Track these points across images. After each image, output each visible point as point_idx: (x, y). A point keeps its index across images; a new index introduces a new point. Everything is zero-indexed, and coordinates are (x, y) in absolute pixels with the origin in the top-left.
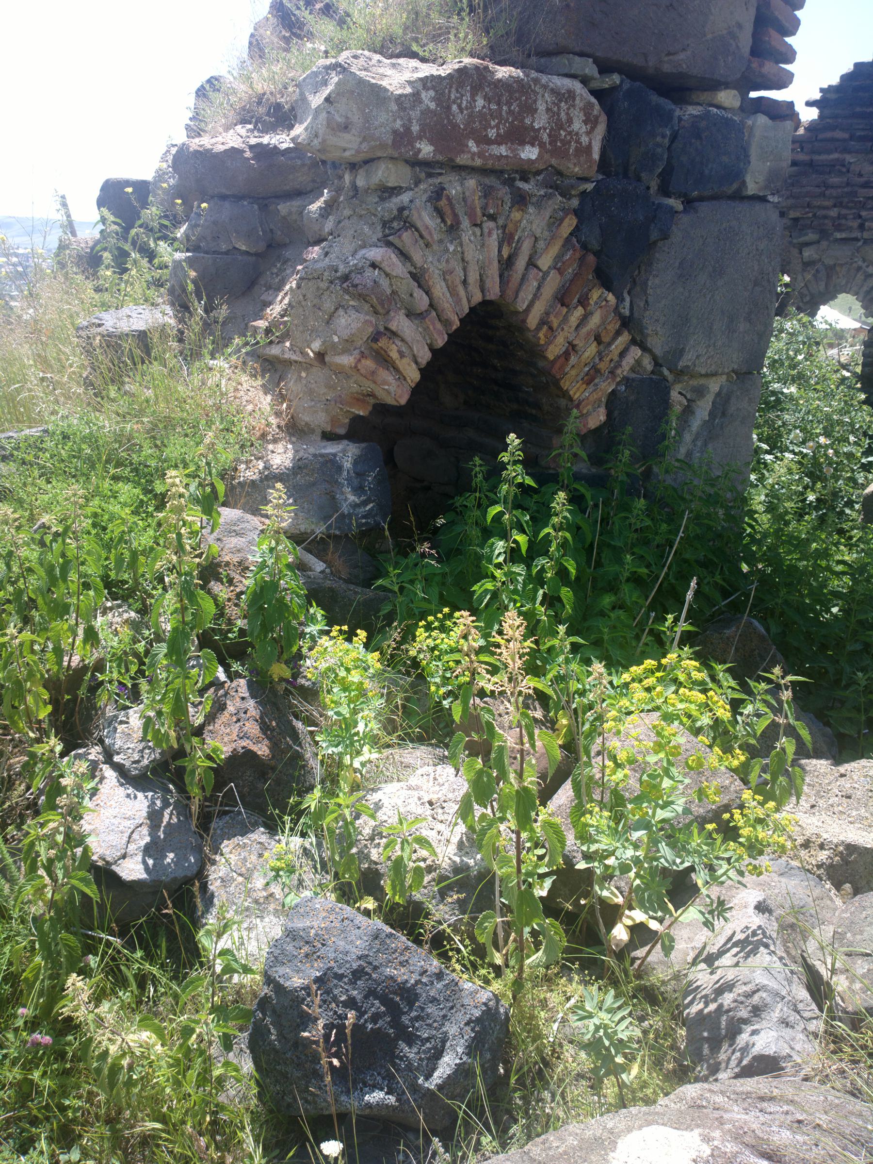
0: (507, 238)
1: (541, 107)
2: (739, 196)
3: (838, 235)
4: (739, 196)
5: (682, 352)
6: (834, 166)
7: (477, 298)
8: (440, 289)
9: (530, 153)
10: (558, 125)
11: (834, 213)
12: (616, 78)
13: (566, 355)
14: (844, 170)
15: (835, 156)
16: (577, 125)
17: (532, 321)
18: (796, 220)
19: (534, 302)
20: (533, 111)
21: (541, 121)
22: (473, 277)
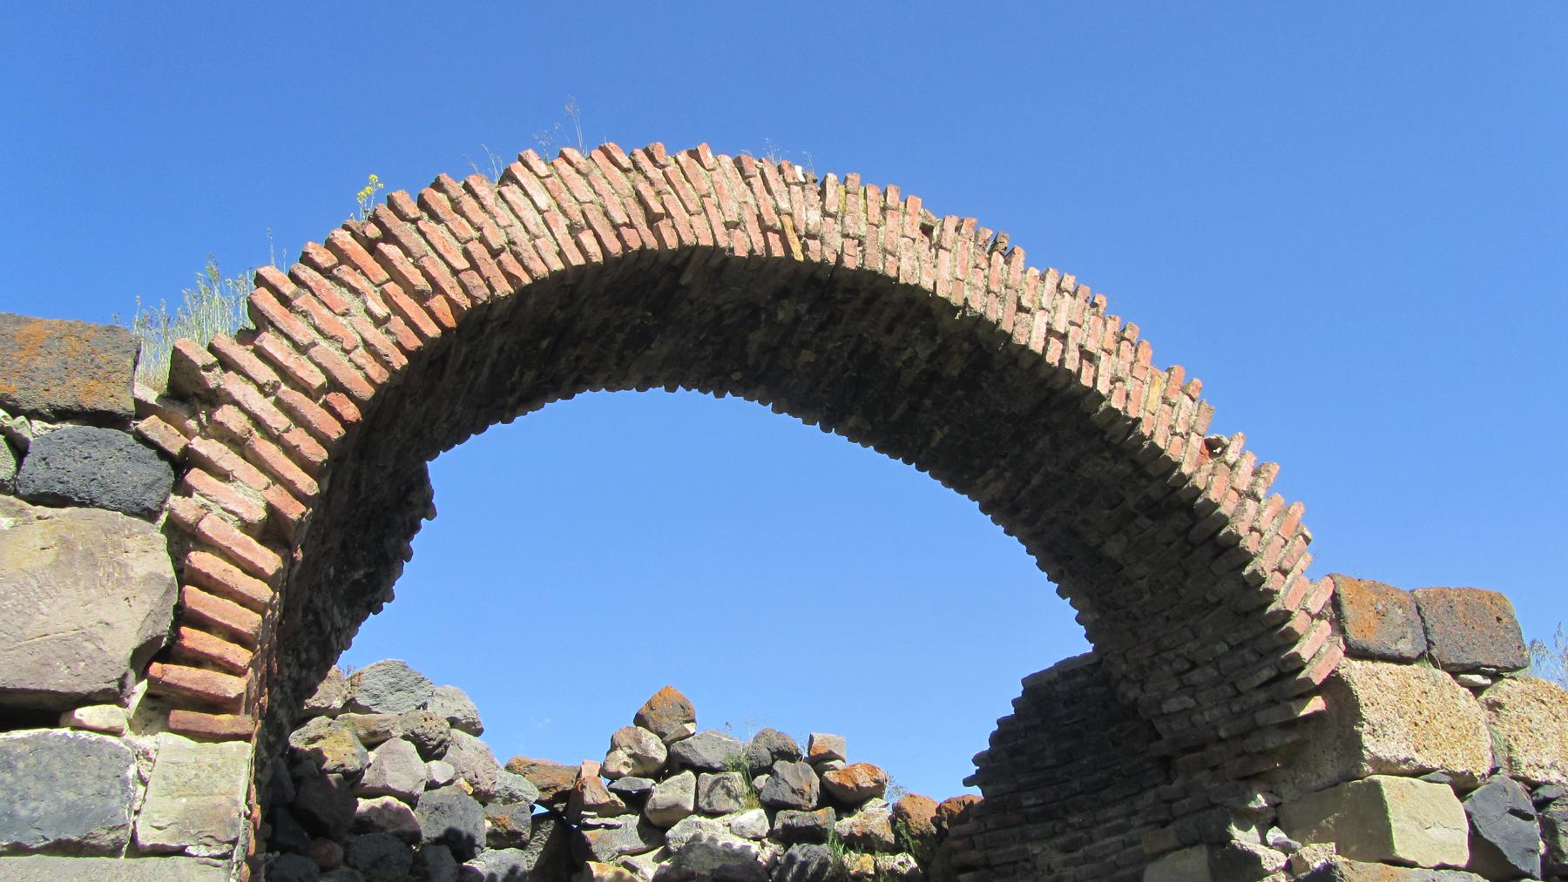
6: (1016, 862)
14: (1029, 866)
15: (1015, 847)
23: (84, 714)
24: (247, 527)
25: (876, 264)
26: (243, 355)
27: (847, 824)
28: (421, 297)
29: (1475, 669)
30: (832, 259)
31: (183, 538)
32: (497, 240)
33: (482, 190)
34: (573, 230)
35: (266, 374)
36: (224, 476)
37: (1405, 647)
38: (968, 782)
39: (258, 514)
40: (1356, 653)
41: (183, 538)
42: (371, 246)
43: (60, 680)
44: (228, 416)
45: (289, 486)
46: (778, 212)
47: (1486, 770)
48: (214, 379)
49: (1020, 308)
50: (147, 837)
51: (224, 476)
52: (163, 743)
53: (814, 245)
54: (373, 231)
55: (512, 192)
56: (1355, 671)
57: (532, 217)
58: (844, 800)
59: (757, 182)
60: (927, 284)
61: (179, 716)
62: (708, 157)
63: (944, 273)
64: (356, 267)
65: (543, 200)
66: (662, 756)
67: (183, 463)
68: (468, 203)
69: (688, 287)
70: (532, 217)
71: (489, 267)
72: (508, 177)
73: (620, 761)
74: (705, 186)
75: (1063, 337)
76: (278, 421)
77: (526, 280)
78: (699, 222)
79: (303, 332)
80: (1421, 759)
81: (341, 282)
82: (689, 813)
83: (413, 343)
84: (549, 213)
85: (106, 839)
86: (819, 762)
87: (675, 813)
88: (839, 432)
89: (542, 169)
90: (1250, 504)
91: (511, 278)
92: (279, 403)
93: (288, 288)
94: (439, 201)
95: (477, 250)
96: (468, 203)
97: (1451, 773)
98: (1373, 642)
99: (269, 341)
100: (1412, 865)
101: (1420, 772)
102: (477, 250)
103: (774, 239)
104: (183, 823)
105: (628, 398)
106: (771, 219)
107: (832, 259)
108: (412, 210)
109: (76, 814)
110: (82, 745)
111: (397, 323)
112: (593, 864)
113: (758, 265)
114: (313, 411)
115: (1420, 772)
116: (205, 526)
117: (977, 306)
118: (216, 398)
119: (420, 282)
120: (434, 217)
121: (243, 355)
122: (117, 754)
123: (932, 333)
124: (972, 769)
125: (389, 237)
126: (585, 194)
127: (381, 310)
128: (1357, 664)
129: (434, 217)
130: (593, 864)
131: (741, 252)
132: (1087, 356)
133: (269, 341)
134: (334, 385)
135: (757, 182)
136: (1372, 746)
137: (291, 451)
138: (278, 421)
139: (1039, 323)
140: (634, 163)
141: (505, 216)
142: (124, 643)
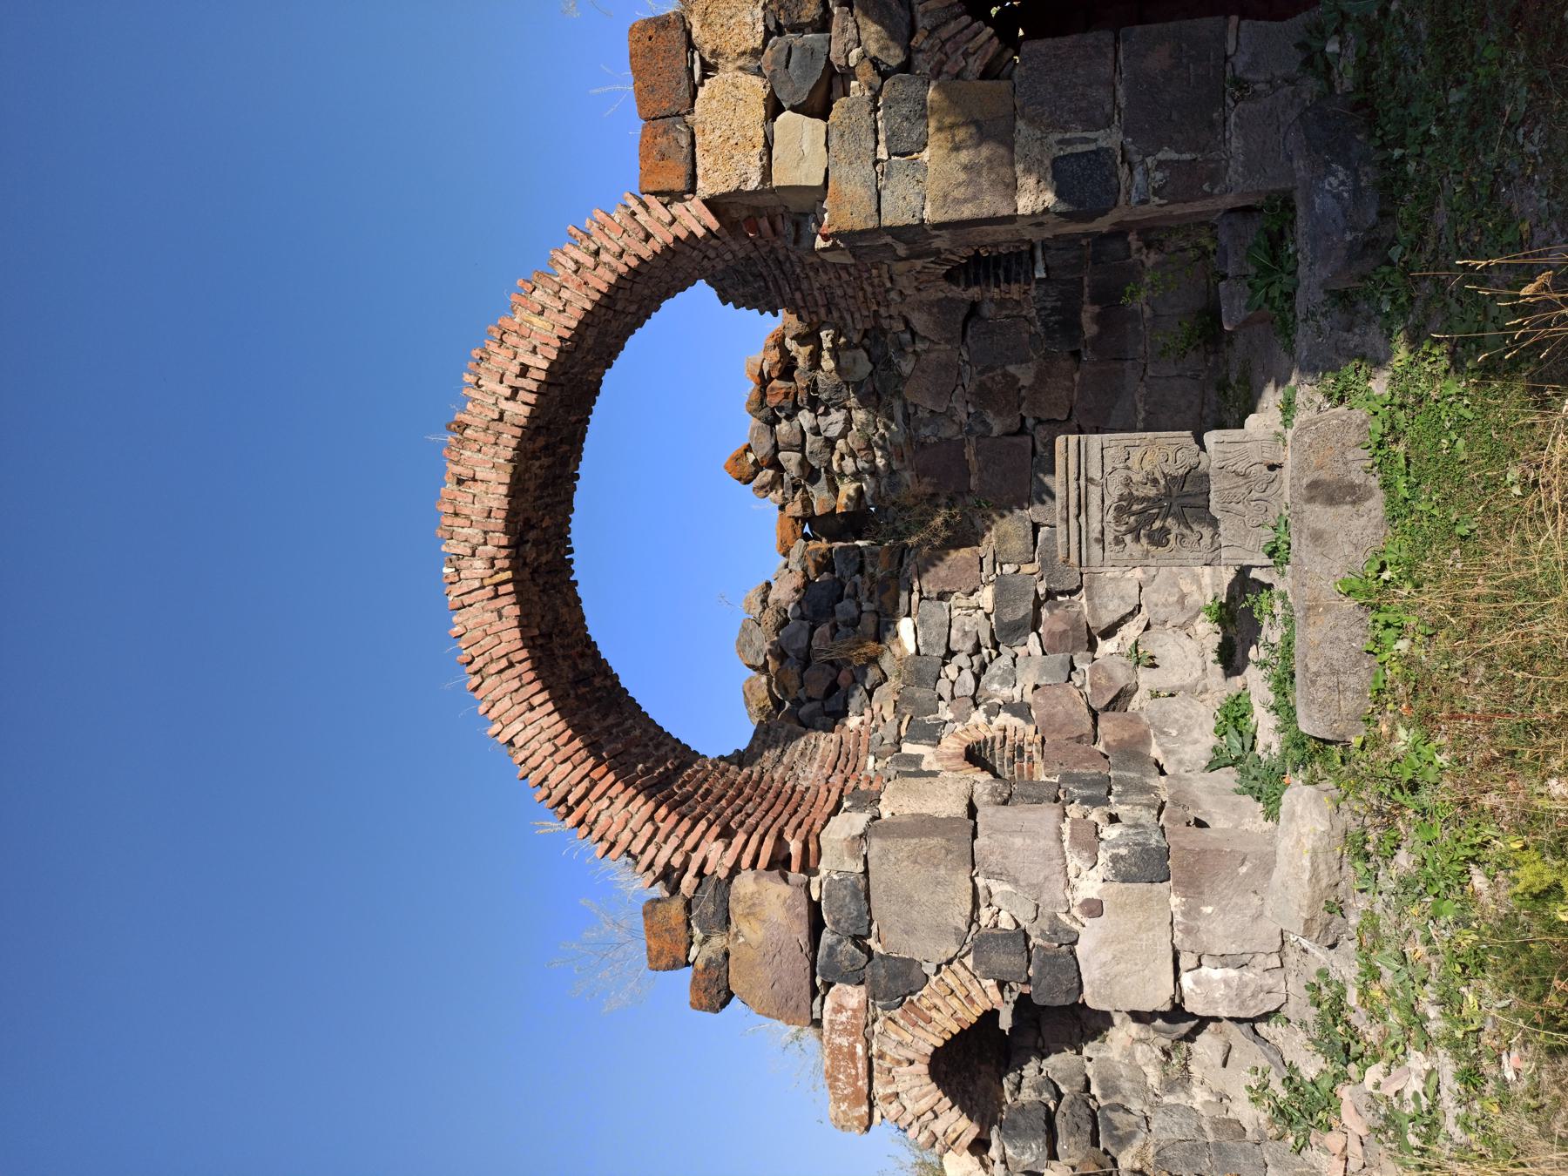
0: (899, 1063)
1: (838, 1041)
2: (866, 872)
3: (889, 285)
4: (866, 872)
5: (956, 929)
7: (928, 1080)
8: (924, 1104)
9: (860, 1049)
10: (846, 1032)
11: (869, 289)
12: (818, 981)
13: (958, 1020)
16: (843, 1017)
17: (940, 1043)
18: (878, 304)
19: (929, 1040)
20: (840, 1047)
21: (844, 1041)
22: (917, 1082)
23: (815, 897)
24: (726, 849)
25: (498, 522)
26: (645, 860)
27: (802, 362)
28: (594, 784)
29: (691, 70)
30: (504, 552)
31: (735, 870)
32: (549, 748)
33: (521, 756)
34: (532, 708)
35: (651, 850)
36: (705, 861)
37: (684, 141)
38: (776, 314)
39: (720, 845)
40: (693, 190)
41: (735, 870)
42: (570, 810)
43: (803, 909)
44: (677, 861)
45: (704, 833)
46: (483, 587)
47: (757, 81)
48: (658, 869)
49: (501, 419)
50: (861, 868)
51: (705, 861)
52: (823, 868)
53: (498, 564)
54: (562, 809)
55: (519, 741)
56: (705, 188)
57: (530, 732)
58: (787, 368)
59: (467, 600)
60: (503, 490)
61: (812, 864)
62: (458, 630)
63: (492, 475)
64: (570, 792)
65: (517, 726)
66: (771, 472)
67: (700, 874)
68: (531, 763)
69: (538, 627)
70: (530, 732)
71: (565, 751)
72: (510, 743)
73: (776, 496)
74: (478, 633)
75: (515, 391)
76: (674, 841)
77: (570, 732)
78: (505, 636)
79: (626, 836)
80: (760, 148)
81: (595, 821)
82: (804, 457)
83: (619, 786)
84: (527, 724)
85: (863, 882)
86: (764, 381)
87: (803, 463)
88: (577, 467)
89: (497, 727)
90: (604, 257)
91: (571, 739)
92: (665, 842)
93: (605, 845)
94: (534, 777)
95: (558, 757)
96: (531, 763)
97: (766, 120)
98: (684, 169)
99: (636, 848)
100: (827, 170)
101: (768, 146)
102: (558, 757)
103: (502, 589)
104: (854, 856)
105: (586, 607)
106: (489, 591)
107: (504, 552)
108: (545, 792)
109: (855, 895)
110: (828, 897)
111: (612, 793)
112: (838, 511)
113: (521, 598)
114: (665, 827)
115: (768, 146)
116: (730, 865)
117: (509, 453)
118: (668, 864)
119: (586, 783)
120: (545, 779)
121: (645, 860)
122: (829, 884)
123: (527, 470)
124: (768, 313)
125: (564, 800)
126: (506, 702)
127: (605, 802)
128: (700, 184)
129: (545, 779)
130: (838, 511)
131: (516, 610)
132: (524, 370)
133: (636, 848)
134: (651, 818)
135: (467, 600)
136: (753, 184)
137: (687, 834)
138: (674, 841)
139: (509, 407)
140: (476, 673)
141: (533, 745)
142: (786, 890)
